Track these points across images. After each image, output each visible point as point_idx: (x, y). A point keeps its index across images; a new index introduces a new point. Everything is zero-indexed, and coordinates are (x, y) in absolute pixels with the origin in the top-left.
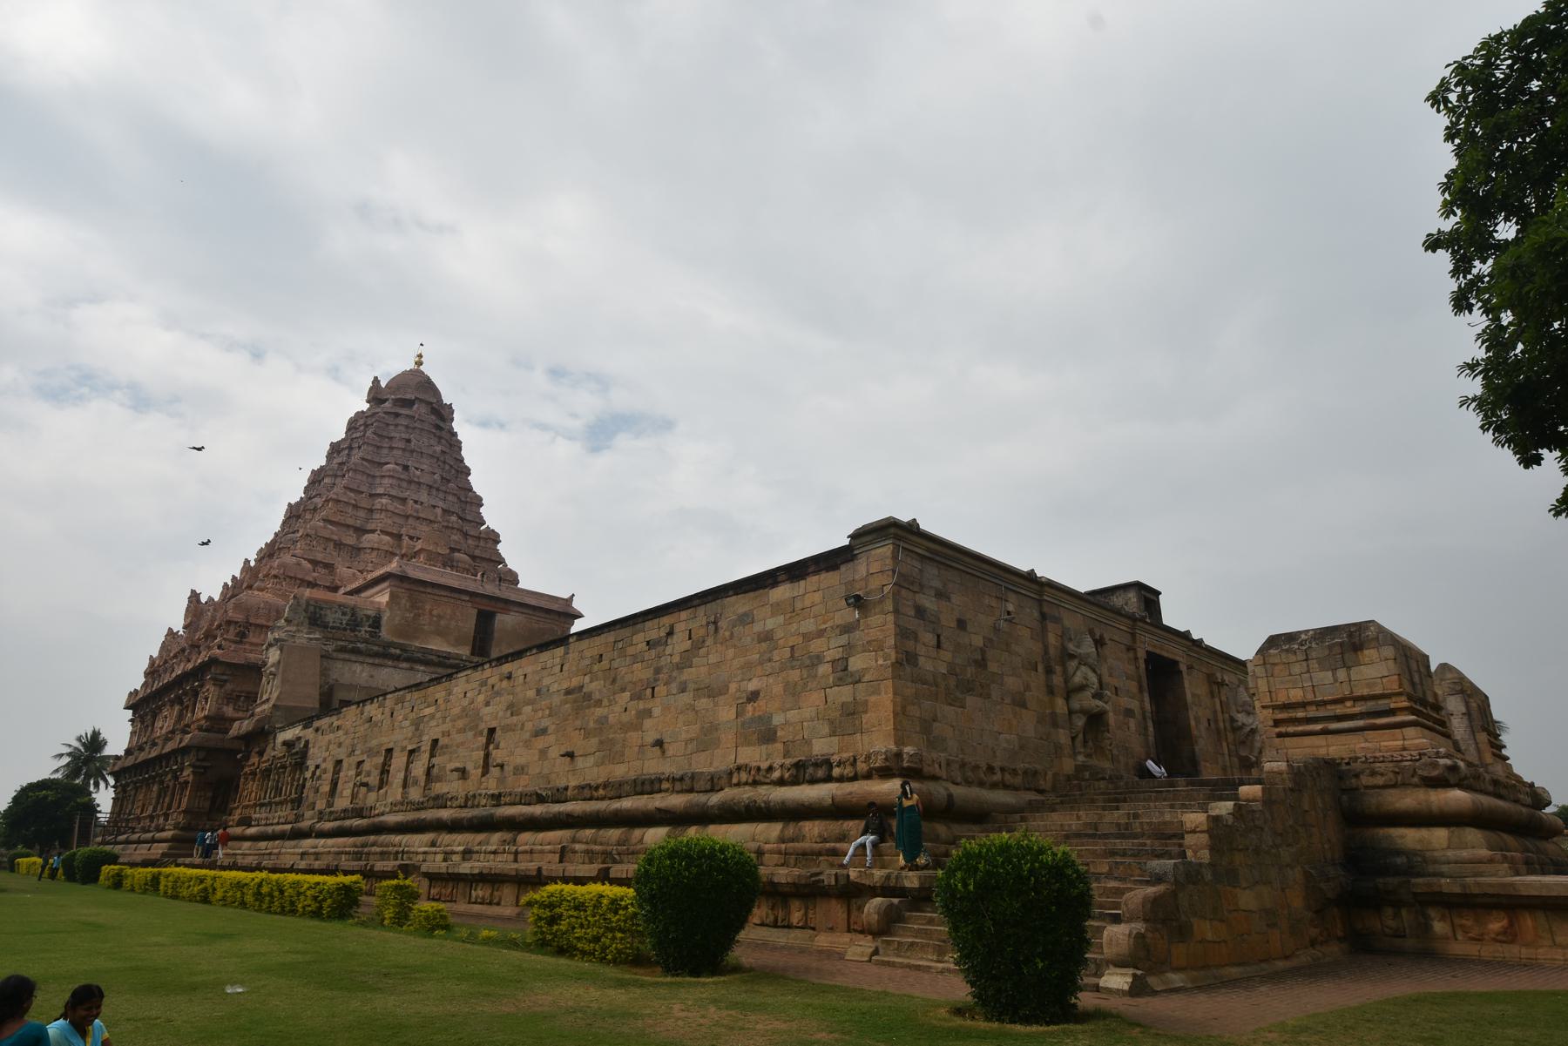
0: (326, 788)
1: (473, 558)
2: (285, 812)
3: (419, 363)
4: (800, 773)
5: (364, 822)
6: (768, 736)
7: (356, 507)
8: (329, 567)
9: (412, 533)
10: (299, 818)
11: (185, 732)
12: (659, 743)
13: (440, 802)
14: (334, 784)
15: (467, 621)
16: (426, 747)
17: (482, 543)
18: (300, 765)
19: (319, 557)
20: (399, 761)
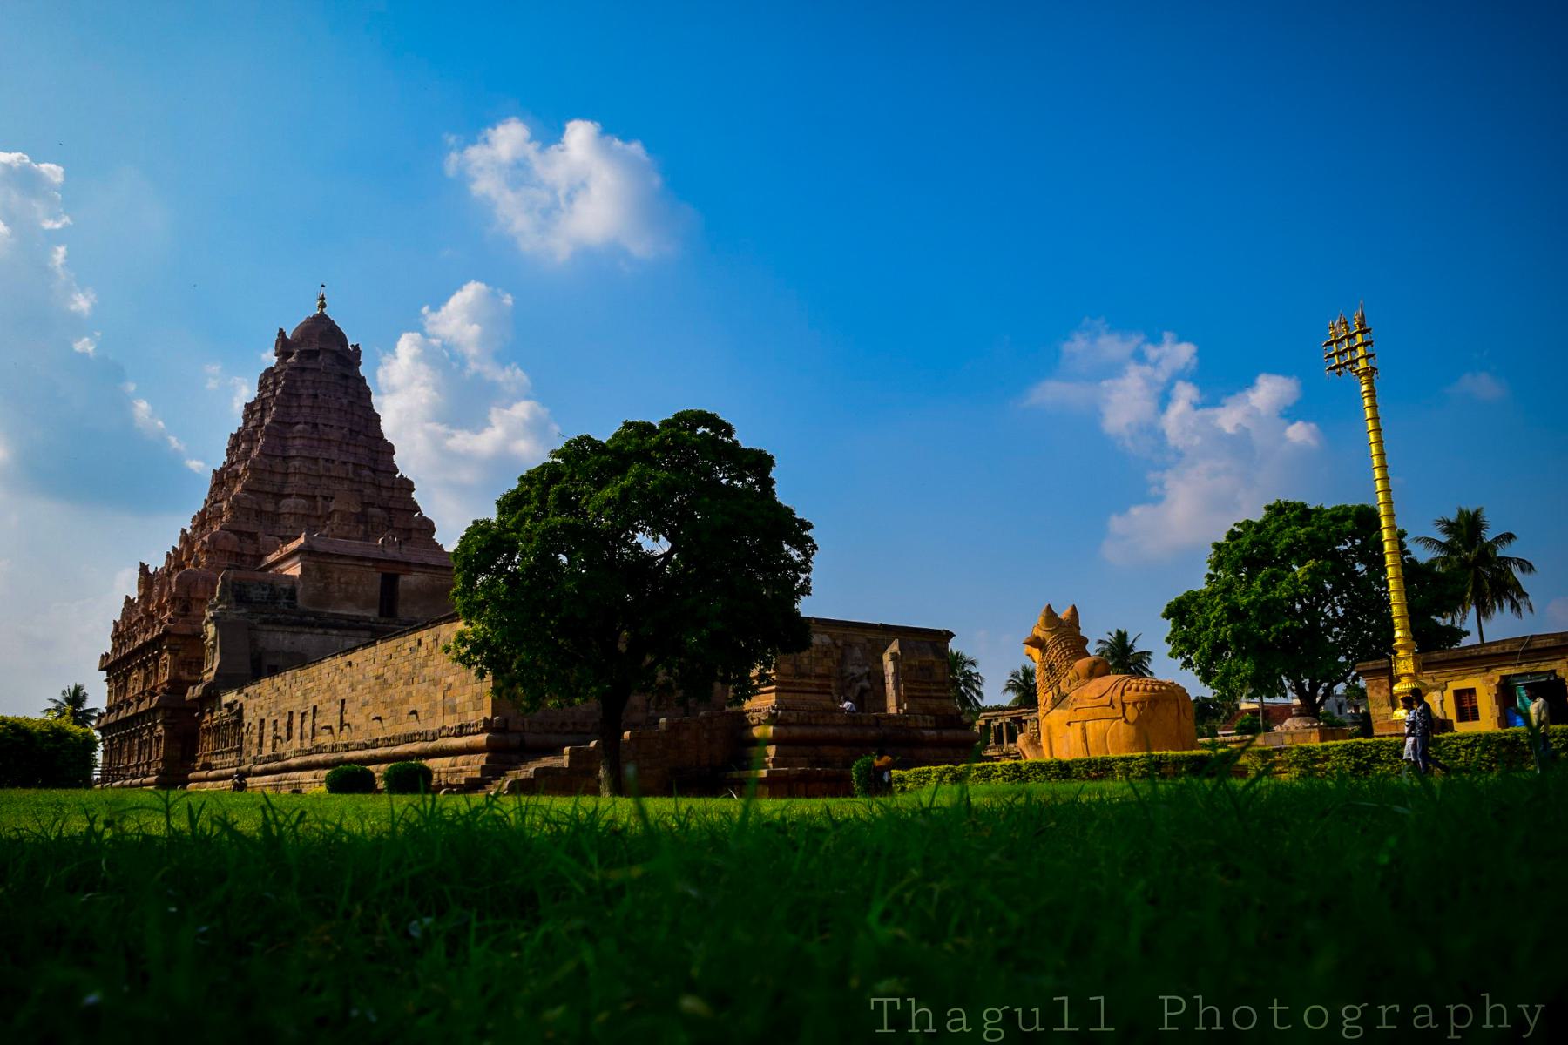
0: (256, 740)
1: (388, 509)
2: (233, 758)
3: (323, 306)
4: (461, 731)
5: (278, 764)
6: (454, 710)
7: (272, 472)
8: (253, 536)
9: (326, 493)
10: (241, 763)
11: (152, 695)
12: (414, 712)
13: (319, 749)
14: (261, 737)
15: (372, 582)
16: (311, 711)
17: (396, 494)
18: (239, 723)
19: (244, 528)
20: (297, 721)
